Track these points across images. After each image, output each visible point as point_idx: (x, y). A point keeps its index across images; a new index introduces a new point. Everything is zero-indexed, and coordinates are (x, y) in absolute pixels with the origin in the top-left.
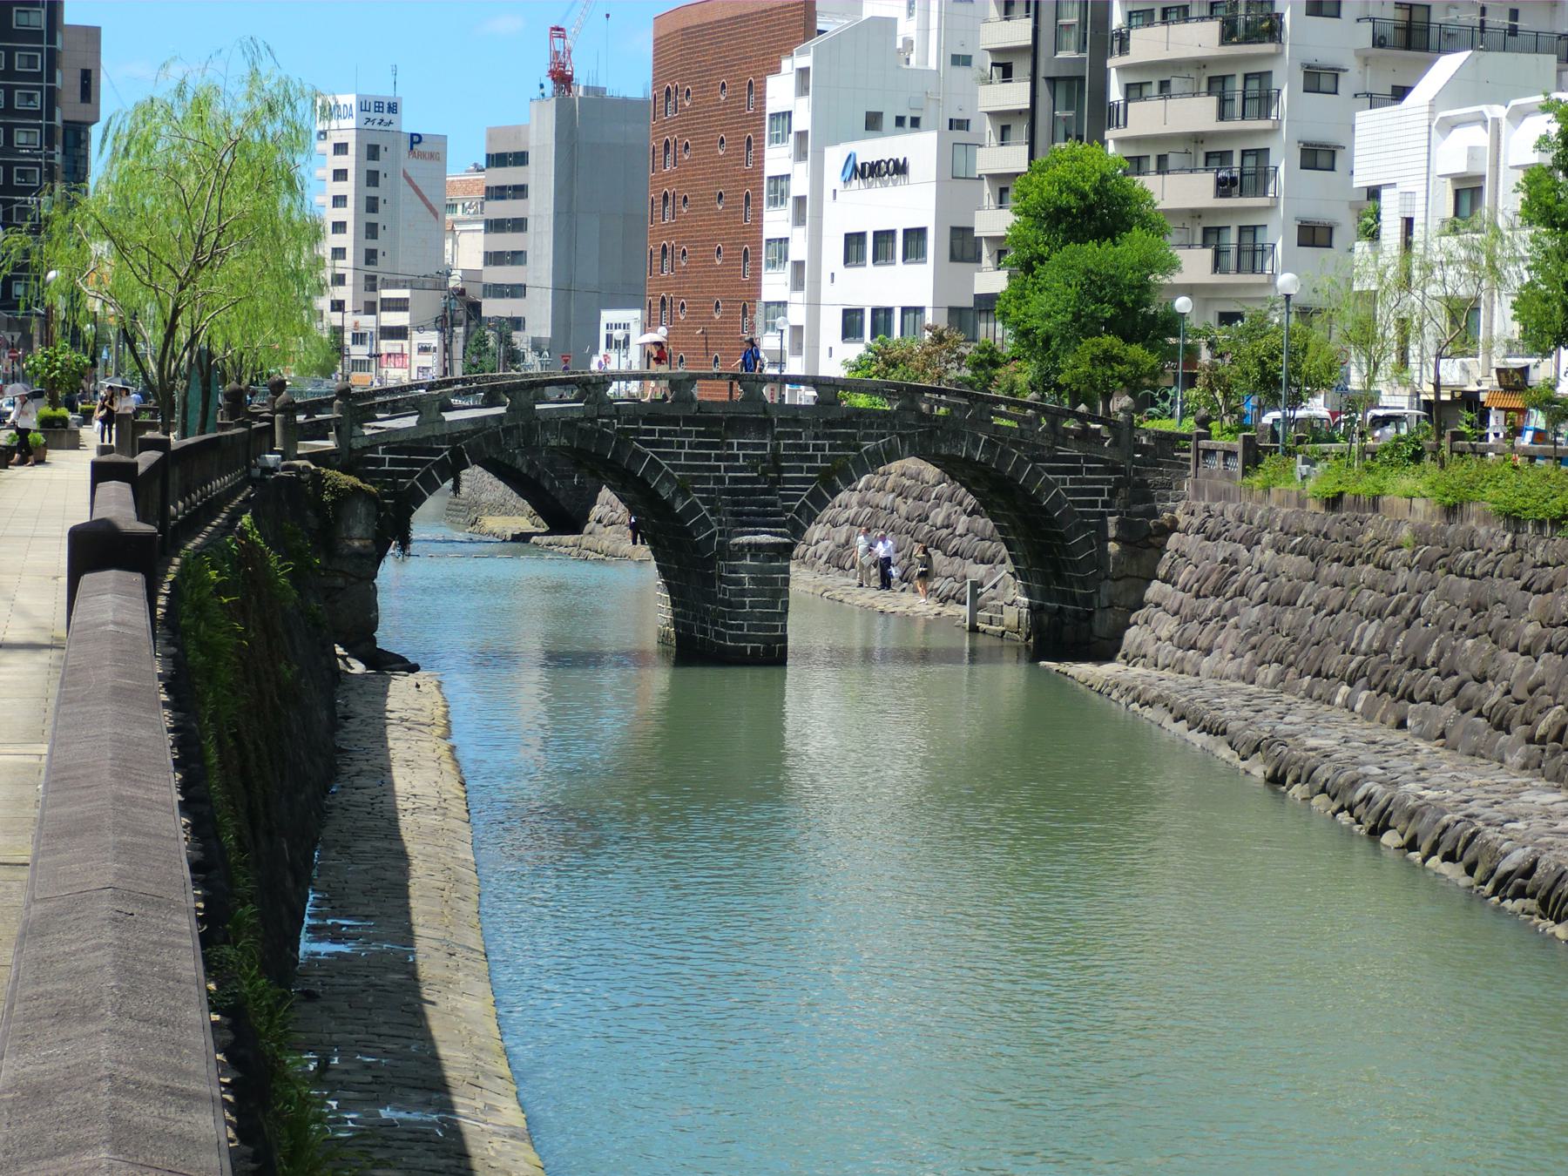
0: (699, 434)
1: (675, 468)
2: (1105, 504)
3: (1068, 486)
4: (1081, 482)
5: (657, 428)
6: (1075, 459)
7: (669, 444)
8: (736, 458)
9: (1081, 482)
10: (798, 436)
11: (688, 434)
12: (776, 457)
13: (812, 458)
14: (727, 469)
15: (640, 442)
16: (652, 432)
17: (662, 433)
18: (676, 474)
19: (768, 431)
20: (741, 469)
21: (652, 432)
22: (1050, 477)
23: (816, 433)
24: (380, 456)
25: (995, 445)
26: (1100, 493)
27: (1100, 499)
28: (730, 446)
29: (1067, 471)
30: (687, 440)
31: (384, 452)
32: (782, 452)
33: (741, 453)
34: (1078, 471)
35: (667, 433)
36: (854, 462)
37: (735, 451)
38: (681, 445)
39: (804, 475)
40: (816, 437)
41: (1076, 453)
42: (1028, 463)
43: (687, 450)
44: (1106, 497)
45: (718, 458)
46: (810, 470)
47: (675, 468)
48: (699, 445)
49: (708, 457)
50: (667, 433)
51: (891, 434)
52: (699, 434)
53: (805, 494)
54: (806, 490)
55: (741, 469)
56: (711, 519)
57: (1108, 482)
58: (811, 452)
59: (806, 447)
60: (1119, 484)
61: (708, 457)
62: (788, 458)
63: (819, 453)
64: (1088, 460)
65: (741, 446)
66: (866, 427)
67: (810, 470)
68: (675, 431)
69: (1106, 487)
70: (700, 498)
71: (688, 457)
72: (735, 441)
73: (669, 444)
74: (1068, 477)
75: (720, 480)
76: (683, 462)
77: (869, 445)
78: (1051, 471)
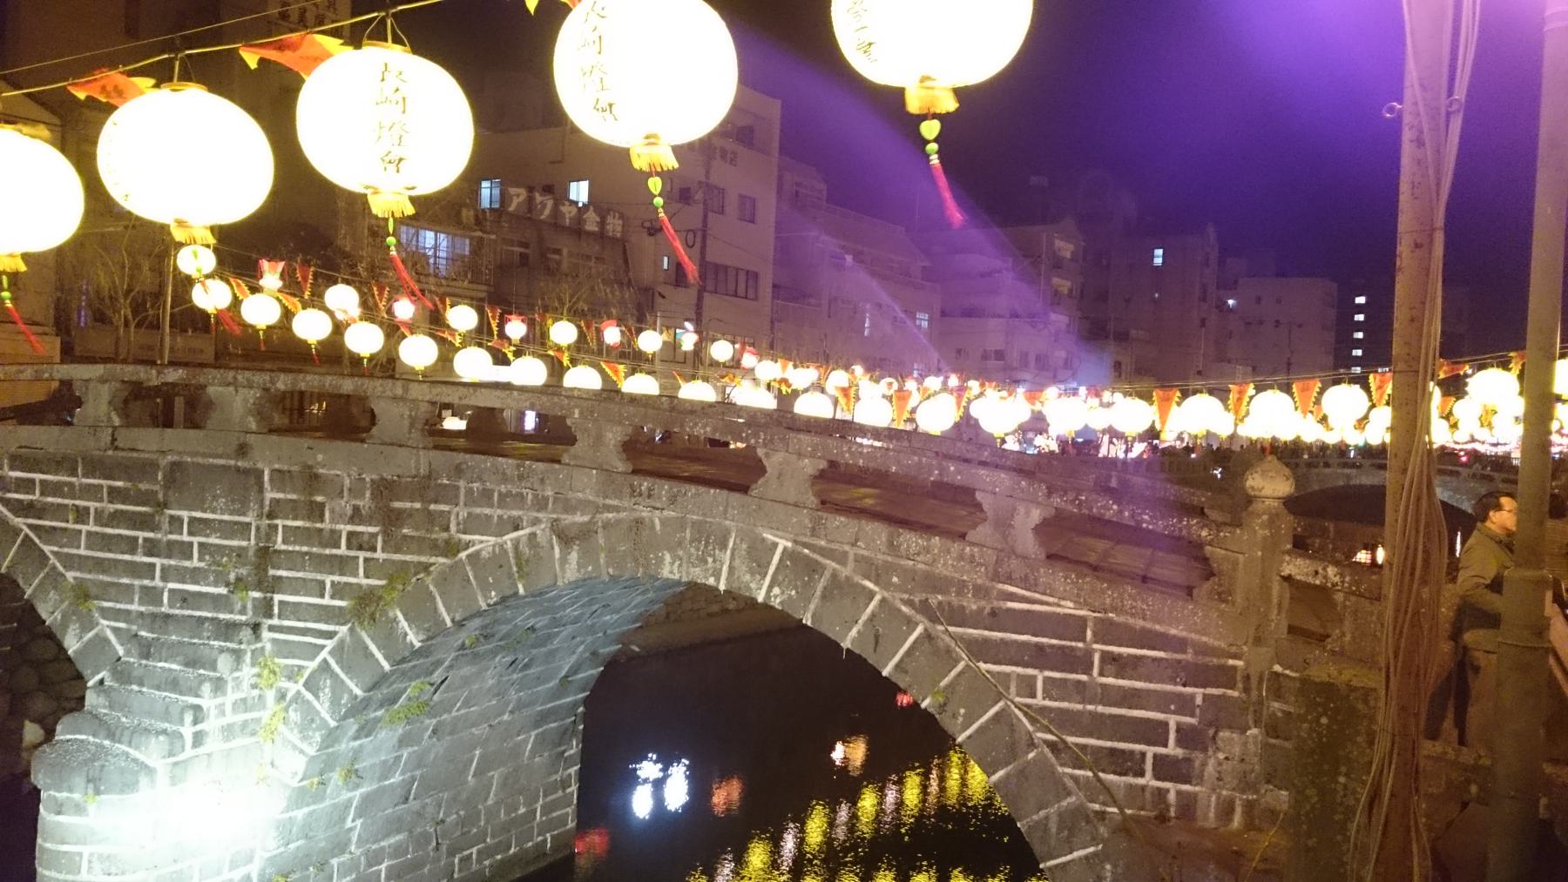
1: (70, 562)
2: (1165, 769)
3: (1039, 701)
4: (1081, 692)
5: (38, 476)
6: (1073, 627)
7: (59, 512)
8: (185, 550)
9: (1081, 692)
10: (316, 512)
11: (92, 492)
12: (266, 555)
13: (344, 565)
16: (27, 485)
17: (47, 488)
18: (70, 575)
19: (253, 495)
20: (195, 575)
21: (27, 485)
23: (356, 509)
25: (814, 569)
27: (1151, 751)
28: (176, 522)
29: (1039, 656)
30: (92, 505)
32: (280, 546)
33: (196, 540)
35: (56, 489)
36: (444, 580)
37: (186, 538)
38: (82, 513)
39: (327, 601)
41: (1068, 608)
42: (912, 624)
44: (1172, 749)
45: (152, 548)
46: (338, 591)
48: (115, 519)
50: (56, 489)
51: (535, 522)
52: (115, 495)
54: (330, 635)
57: (1185, 705)
58: (343, 550)
60: (1220, 716)
62: (293, 560)
63: (362, 555)
64: (1107, 632)
65: (197, 526)
66: (471, 500)
68: (71, 485)
69: (1173, 720)
70: (115, 630)
72: (185, 514)
73: (59, 512)
74: (1040, 676)
75: (151, 595)
76: (83, 552)
77: (484, 543)
78: (980, 650)
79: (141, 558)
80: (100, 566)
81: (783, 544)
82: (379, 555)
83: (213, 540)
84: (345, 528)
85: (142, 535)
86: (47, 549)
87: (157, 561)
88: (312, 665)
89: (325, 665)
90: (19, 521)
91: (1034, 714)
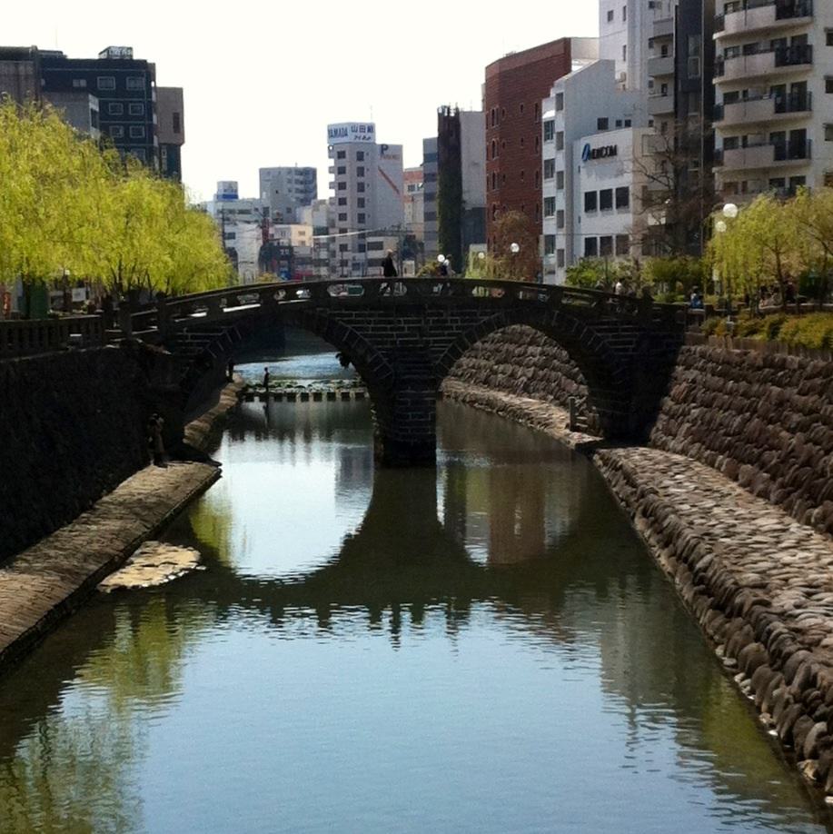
0: (380, 315)
1: (365, 336)
2: (634, 350)
6: (615, 323)
7: (362, 322)
8: (403, 328)
11: (370, 315)
14: (398, 336)
15: (343, 321)
20: (406, 336)
22: (599, 335)
24: (185, 333)
26: (630, 343)
29: (610, 331)
31: (187, 331)
33: (406, 326)
34: (617, 330)
37: (402, 325)
38: (369, 323)
40: (452, 315)
43: (372, 325)
45: (392, 329)
46: (449, 335)
47: (365, 336)
48: (380, 322)
49: (385, 329)
52: (380, 315)
53: (447, 349)
55: (406, 336)
56: (390, 366)
59: (446, 321)
61: (385, 329)
65: (405, 322)
67: (449, 335)
71: (373, 329)
78: (599, 331)
79: (390, 333)
80: (375, 336)
81: (558, 312)
82: (459, 324)
83: (411, 325)
84: (449, 318)
85: (389, 326)
86: (358, 333)
87: (394, 333)
88: (442, 355)
89: (446, 355)
90: (349, 326)
91: (610, 343)
